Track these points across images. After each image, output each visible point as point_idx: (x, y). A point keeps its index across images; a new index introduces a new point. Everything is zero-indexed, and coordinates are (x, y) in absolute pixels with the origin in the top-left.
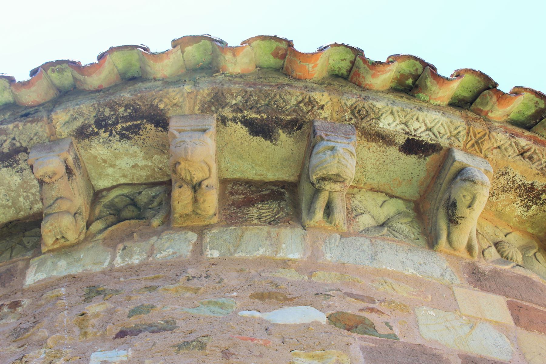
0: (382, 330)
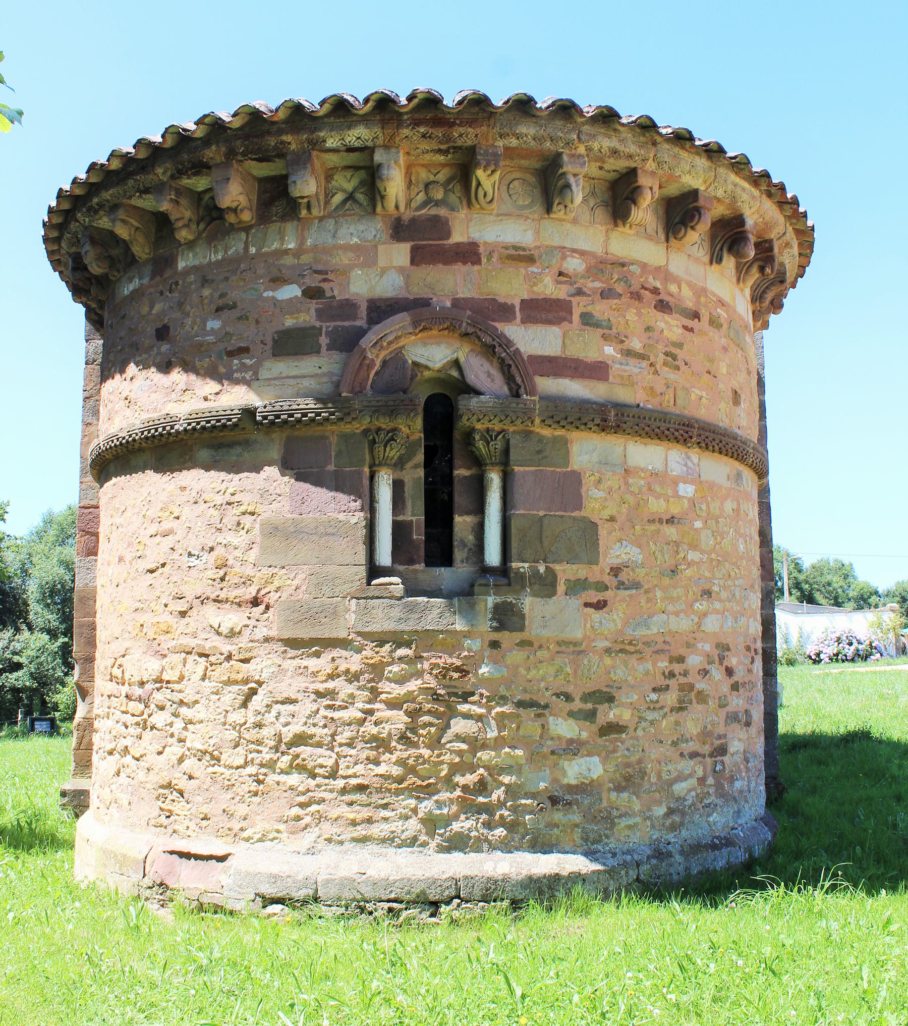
0: (328, 294)
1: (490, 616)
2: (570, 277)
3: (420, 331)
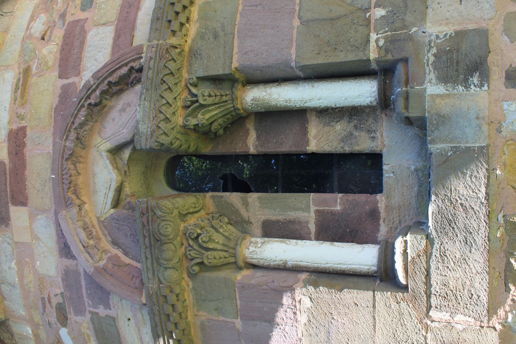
0: (61, 300)
1: (461, 88)
2: (49, 28)
3: (78, 198)
